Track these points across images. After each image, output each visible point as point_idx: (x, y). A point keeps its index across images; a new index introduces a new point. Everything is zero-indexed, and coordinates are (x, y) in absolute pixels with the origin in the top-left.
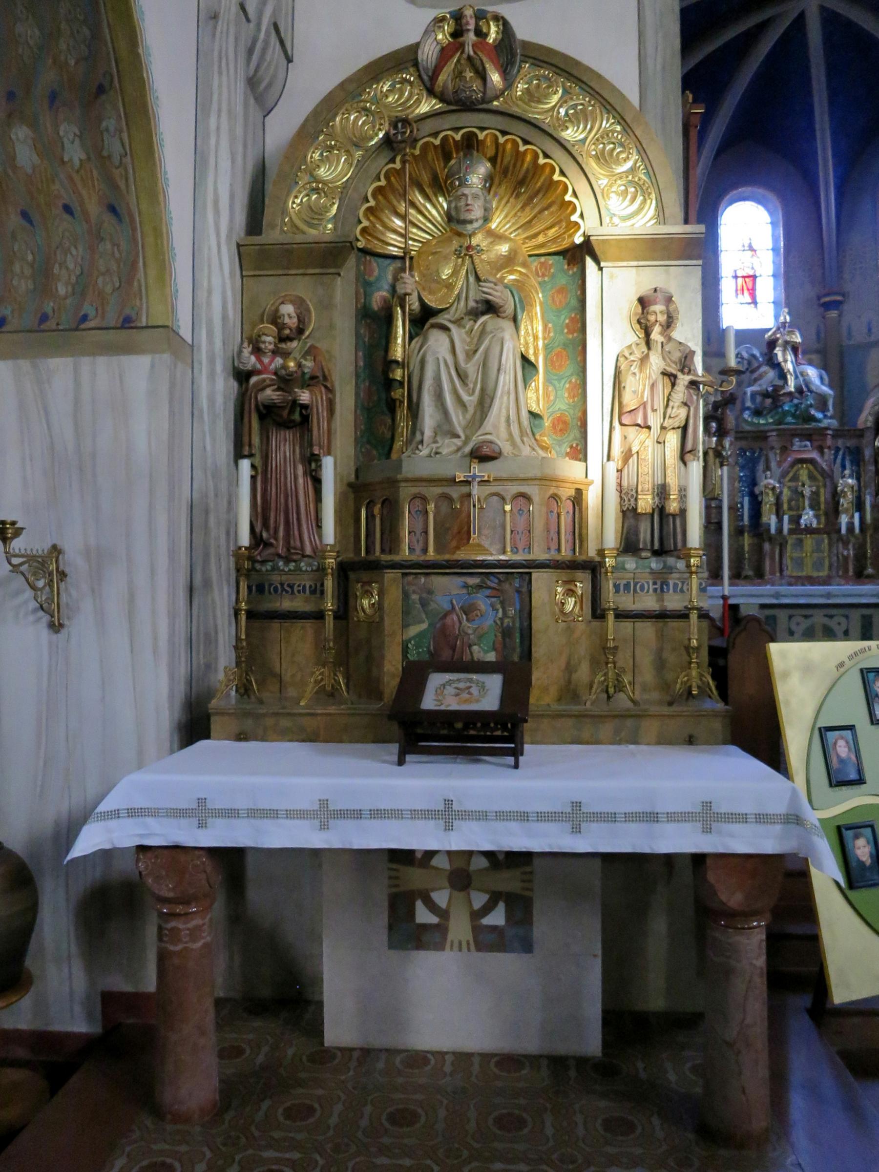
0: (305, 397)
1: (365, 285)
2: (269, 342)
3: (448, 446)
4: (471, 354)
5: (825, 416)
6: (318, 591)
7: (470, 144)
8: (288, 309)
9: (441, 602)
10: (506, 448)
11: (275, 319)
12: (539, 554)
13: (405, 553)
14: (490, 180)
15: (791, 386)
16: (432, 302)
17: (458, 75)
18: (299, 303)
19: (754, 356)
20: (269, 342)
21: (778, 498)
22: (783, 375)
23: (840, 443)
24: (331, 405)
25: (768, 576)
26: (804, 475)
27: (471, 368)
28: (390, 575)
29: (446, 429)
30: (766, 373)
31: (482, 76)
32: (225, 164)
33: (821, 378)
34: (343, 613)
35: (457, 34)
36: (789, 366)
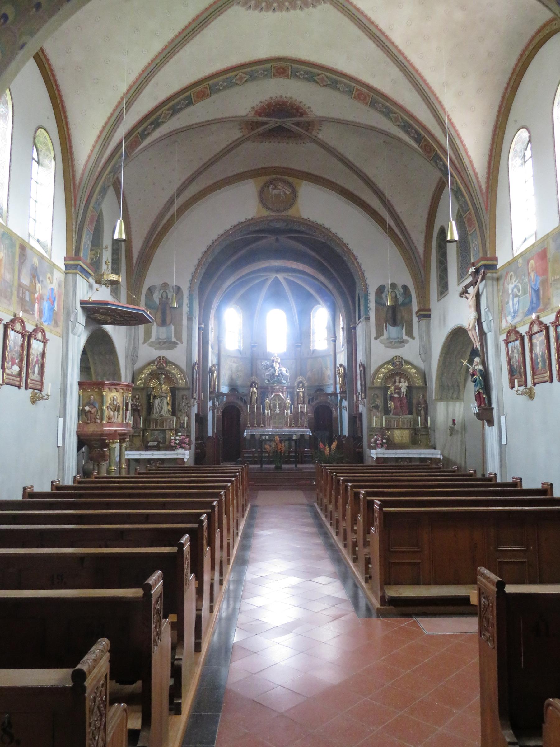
0: (139, 408)
1: (148, 392)
2: (134, 401)
3: (157, 415)
4: (160, 402)
5: (287, 382)
6: (140, 433)
7: (162, 373)
8: (137, 396)
9: (155, 434)
10: (164, 415)
11: (135, 397)
12: (168, 428)
13: (151, 428)
14: (165, 378)
15: (277, 374)
16: (156, 395)
17: (160, 365)
18: (138, 395)
19: (268, 365)
20: (134, 401)
21: (270, 405)
22: (275, 371)
23: (288, 390)
24: (143, 409)
25: (266, 426)
26: (277, 399)
27: (160, 405)
28: (149, 431)
29: (157, 412)
30: (271, 370)
31: (163, 365)
32: (129, 377)
33: (286, 371)
34: (143, 435)
35: (160, 359)
36: (277, 368)
